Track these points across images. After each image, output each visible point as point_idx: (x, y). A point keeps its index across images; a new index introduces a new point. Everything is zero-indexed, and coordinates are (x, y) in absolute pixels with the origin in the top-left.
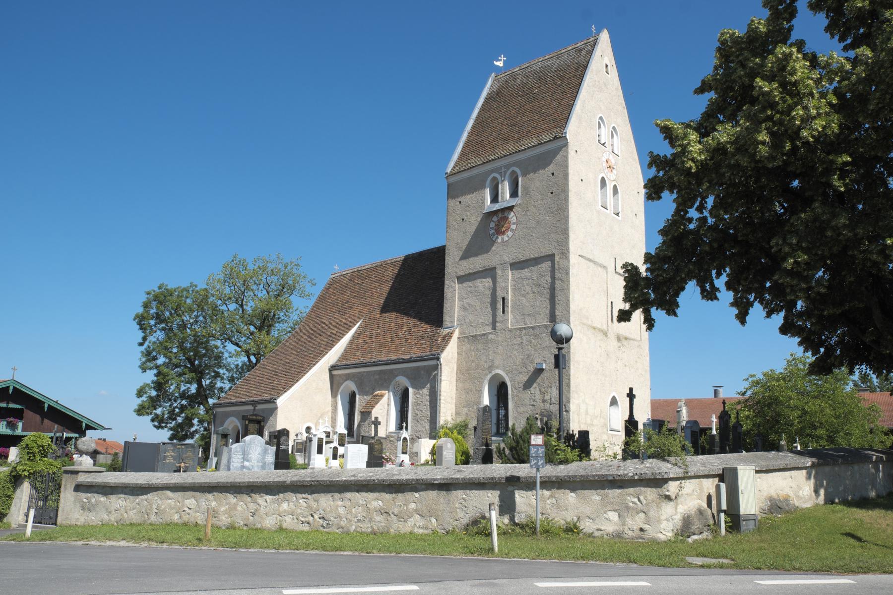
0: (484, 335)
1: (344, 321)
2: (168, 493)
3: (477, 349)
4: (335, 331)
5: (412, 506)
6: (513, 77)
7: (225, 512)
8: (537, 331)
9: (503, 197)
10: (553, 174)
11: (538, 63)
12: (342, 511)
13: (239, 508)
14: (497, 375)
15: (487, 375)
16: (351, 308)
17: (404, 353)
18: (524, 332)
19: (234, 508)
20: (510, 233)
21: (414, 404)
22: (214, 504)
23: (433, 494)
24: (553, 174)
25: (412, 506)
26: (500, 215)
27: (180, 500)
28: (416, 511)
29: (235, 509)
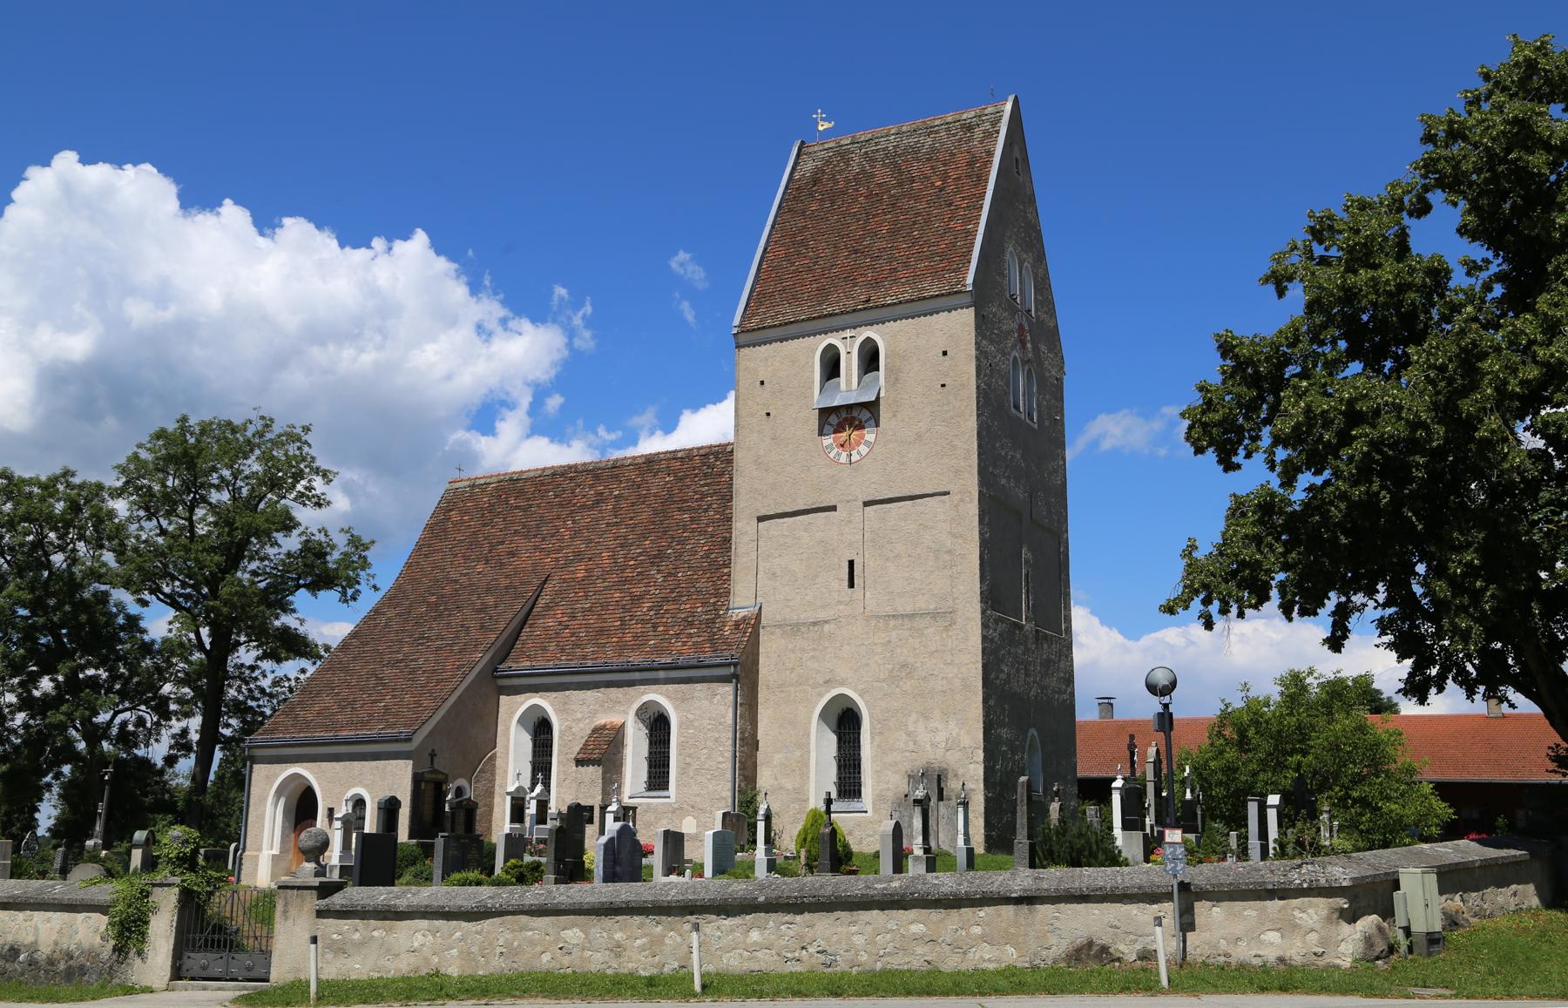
0: (815, 624)
1: (504, 582)
2: (524, 919)
3: (803, 650)
4: (491, 600)
5: (977, 930)
6: (843, 154)
7: (642, 949)
8: (920, 623)
9: (849, 382)
10: (945, 353)
11: (890, 134)
12: (859, 940)
13: (667, 941)
14: (842, 697)
15: (821, 695)
16: (512, 554)
17: (658, 650)
18: (892, 623)
19: (660, 940)
20: (863, 449)
21: (681, 746)
22: (618, 936)
23: (1008, 911)
24: (945, 353)
25: (977, 930)
26: (844, 415)
27: (550, 931)
28: (983, 938)
29: (662, 943)
